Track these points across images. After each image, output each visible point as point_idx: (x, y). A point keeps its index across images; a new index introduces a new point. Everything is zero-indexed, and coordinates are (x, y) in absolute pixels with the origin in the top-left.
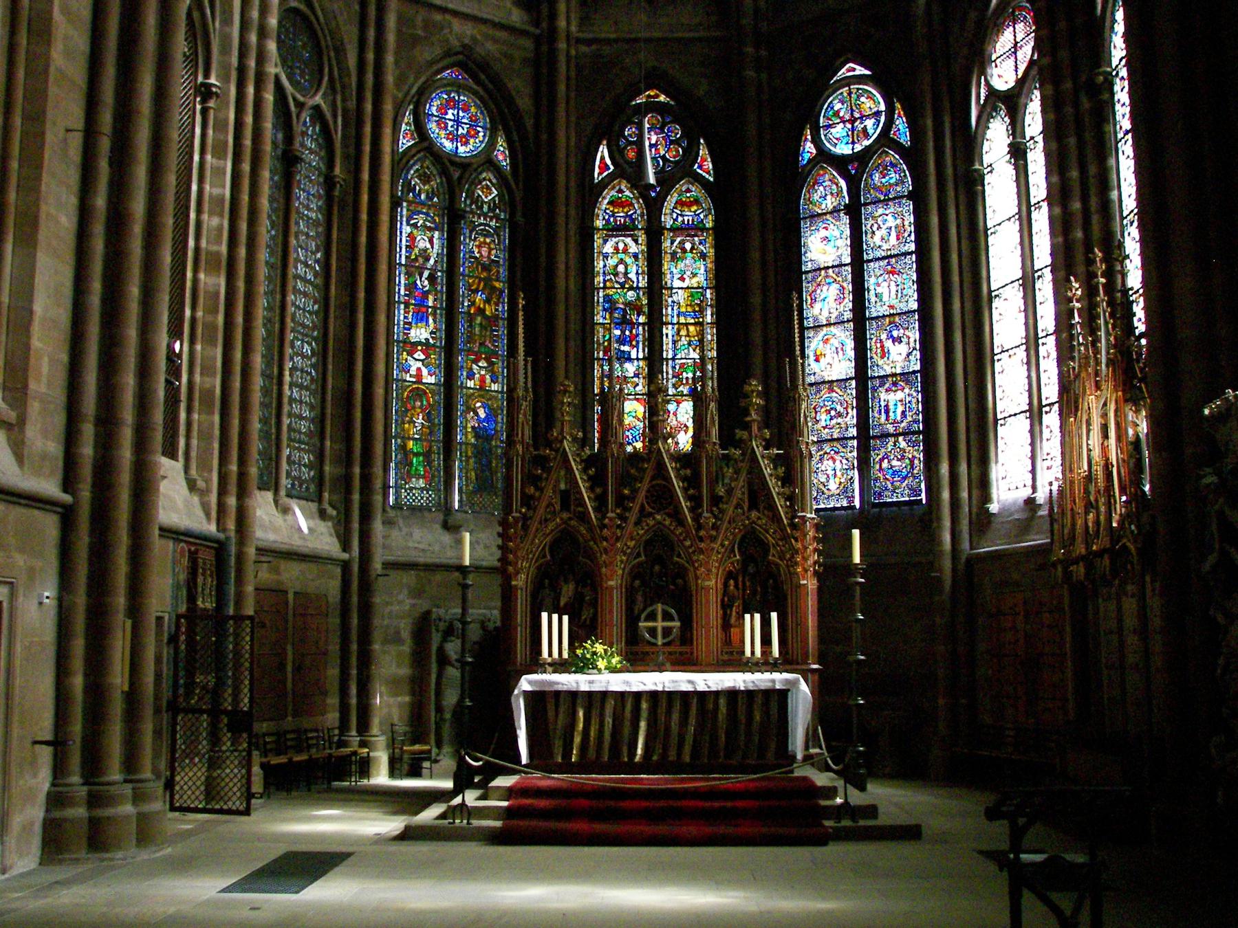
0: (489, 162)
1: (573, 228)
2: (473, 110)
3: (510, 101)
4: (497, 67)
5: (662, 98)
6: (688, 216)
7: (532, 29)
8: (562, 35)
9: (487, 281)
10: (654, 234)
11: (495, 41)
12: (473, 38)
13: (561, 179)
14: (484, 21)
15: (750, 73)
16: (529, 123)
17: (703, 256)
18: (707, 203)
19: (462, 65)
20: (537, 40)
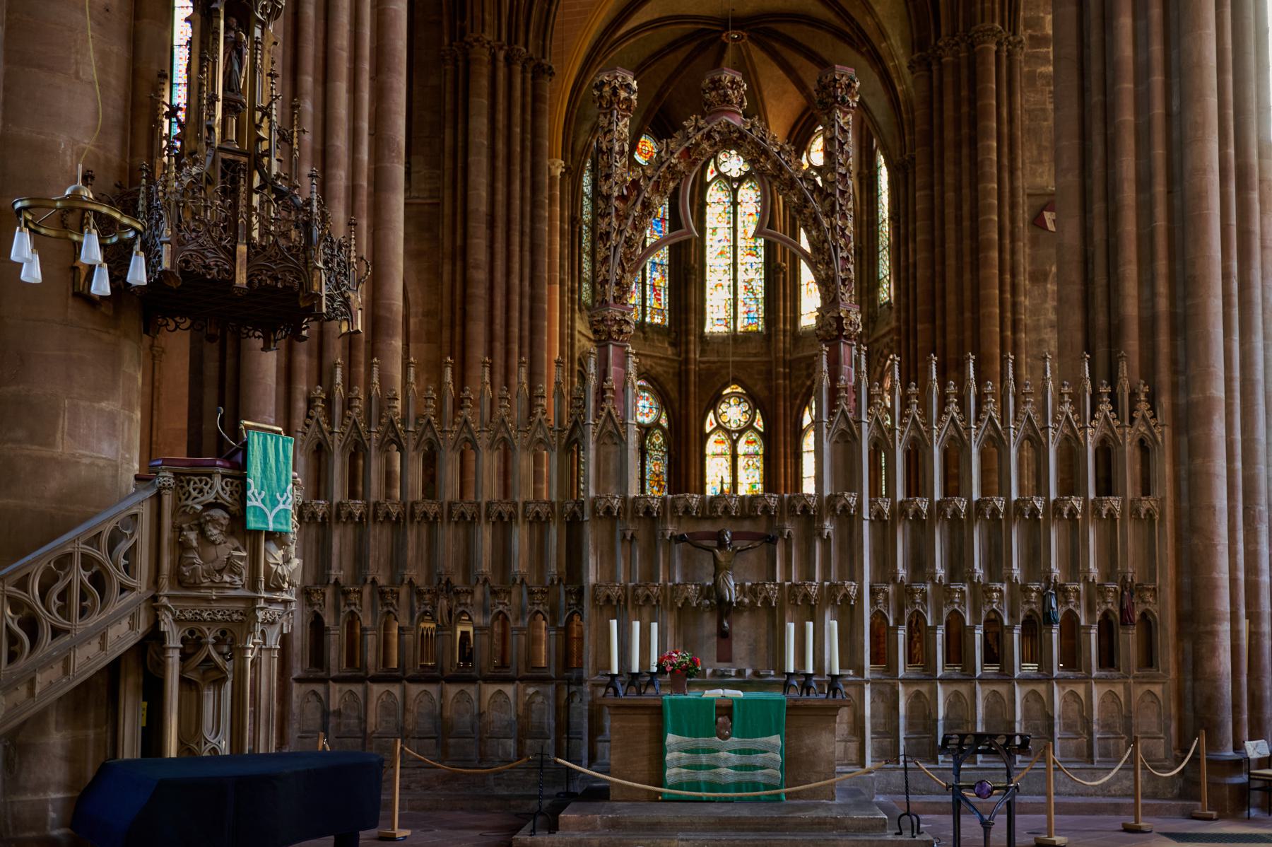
0: (656, 424)
1: (698, 455)
2: (651, 400)
3: (667, 394)
4: (661, 379)
5: (740, 390)
6: (751, 449)
7: (675, 358)
8: (693, 361)
9: (658, 481)
10: (734, 457)
11: (661, 365)
12: (651, 366)
13: (692, 433)
14: (656, 357)
15: (781, 381)
16: (677, 405)
17: (758, 468)
18: (760, 442)
19: (646, 379)
20: (680, 363)
